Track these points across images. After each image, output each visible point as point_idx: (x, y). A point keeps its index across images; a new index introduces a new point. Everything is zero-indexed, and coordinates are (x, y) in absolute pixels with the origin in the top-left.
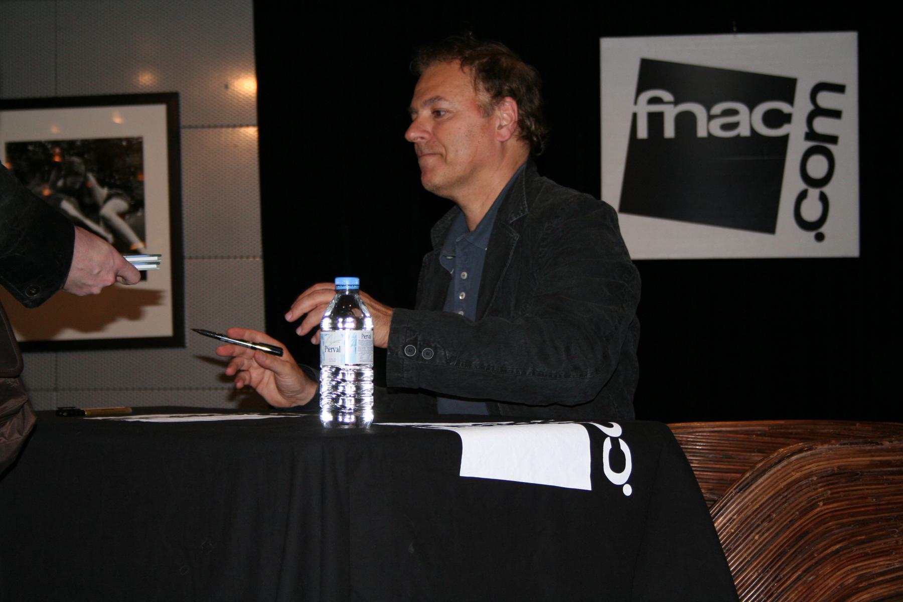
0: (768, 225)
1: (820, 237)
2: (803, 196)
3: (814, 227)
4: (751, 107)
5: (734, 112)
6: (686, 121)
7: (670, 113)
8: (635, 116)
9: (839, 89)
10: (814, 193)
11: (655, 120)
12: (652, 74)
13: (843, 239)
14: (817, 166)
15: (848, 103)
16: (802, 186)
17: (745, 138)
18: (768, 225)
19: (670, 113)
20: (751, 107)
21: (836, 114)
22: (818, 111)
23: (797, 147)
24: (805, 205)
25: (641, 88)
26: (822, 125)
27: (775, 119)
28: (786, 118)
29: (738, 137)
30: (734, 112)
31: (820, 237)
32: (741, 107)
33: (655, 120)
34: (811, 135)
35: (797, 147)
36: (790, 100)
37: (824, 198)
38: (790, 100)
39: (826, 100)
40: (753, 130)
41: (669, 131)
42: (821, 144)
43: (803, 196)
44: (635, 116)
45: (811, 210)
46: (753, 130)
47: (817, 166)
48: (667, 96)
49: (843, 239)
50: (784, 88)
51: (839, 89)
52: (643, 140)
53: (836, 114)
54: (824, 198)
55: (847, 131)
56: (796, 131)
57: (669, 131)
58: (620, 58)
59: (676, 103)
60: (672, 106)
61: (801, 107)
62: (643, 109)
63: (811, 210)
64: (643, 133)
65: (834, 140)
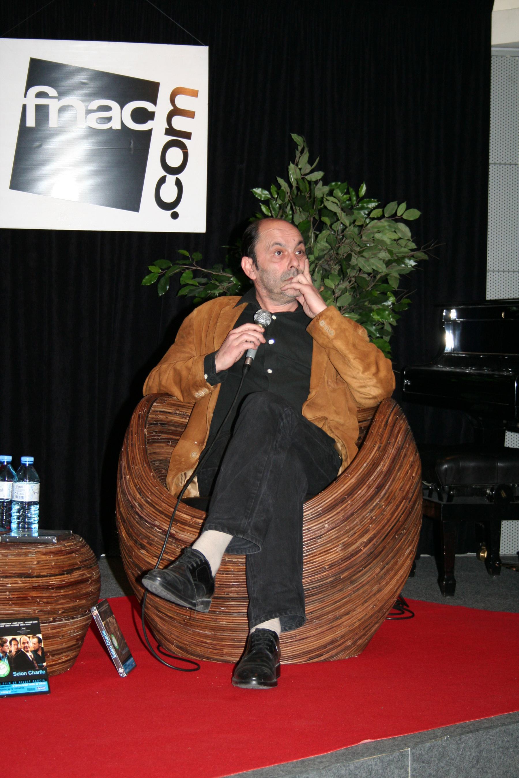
0: (133, 204)
1: (175, 216)
2: (162, 180)
3: (170, 207)
4: (122, 107)
5: (108, 109)
8: (24, 107)
9: (194, 93)
10: (171, 179)
13: (193, 219)
14: (174, 157)
15: (200, 105)
16: (163, 173)
17: (117, 130)
18: (133, 204)
20: (122, 107)
21: (190, 114)
22: (175, 112)
23: (159, 140)
24: (163, 187)
25: (30, 84)
26: (179, 123)
27: (142, 116)
28: (151, 116)
29: (111, 128)
30: (108, 109)
31: (175, 216)
32: (114, 105)
34: (170, 131)
35: (159, 140)
36: (154, 102)
37: (179, 184)
38: (154, 102)
39: (182, 102)
40: (122, 123)
42: (178, 139)
43: (162, 180)
44: (24, 107)
45: (169, 193)
46: (122, 123)
47: (174, 157)
49: (193, 219)
50: (148, 90)
51: (194, 93)
52: (31, 129)
53: (190, 114)
54: (179, 184)
55: (198, 128)
56: (157, 127)
60: (57, 100)
61: (162, 108)
62: (32, 102)
63: (169, 193)
64: (31, 122)
65: (188, 135)
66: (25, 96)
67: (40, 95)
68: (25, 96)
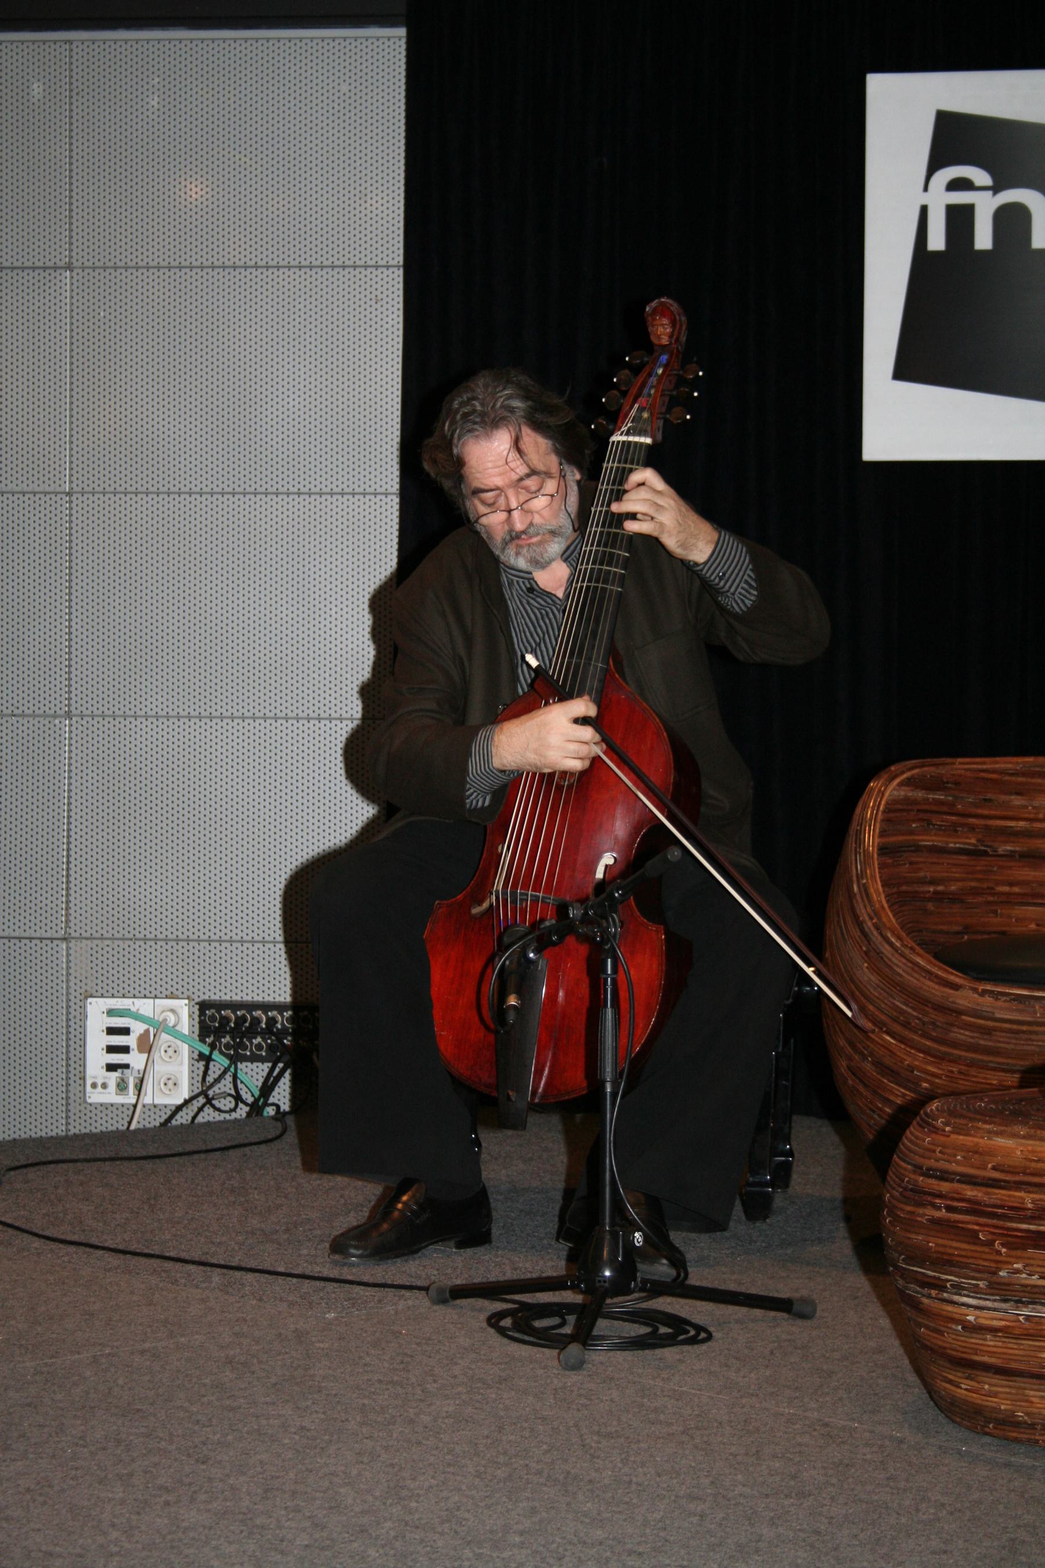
6: (1013, 222)
7: (985, 206)
8: (924, 210)
11: (960, 219)
12: (956, 139)
19: (985, 206)
25: (935, 165)
33: (960, 219)
41: (983, 239)
44: (924, 210)
48: (980, 176)
57: (983, 239)
58: (900, 109)
59: (996, 189)
60: (990, 193)
62: (939, 199)
64: (937, 241)
66: (926, 189)
67: (958, 185)
68: (926, 189)
